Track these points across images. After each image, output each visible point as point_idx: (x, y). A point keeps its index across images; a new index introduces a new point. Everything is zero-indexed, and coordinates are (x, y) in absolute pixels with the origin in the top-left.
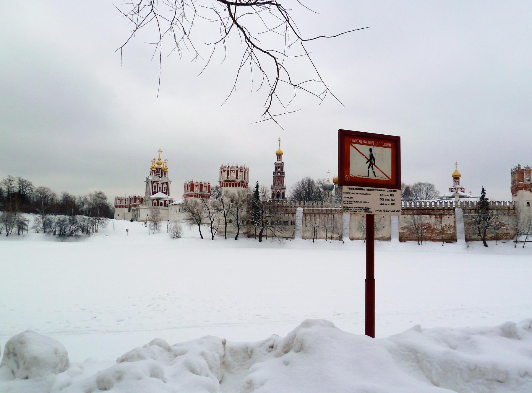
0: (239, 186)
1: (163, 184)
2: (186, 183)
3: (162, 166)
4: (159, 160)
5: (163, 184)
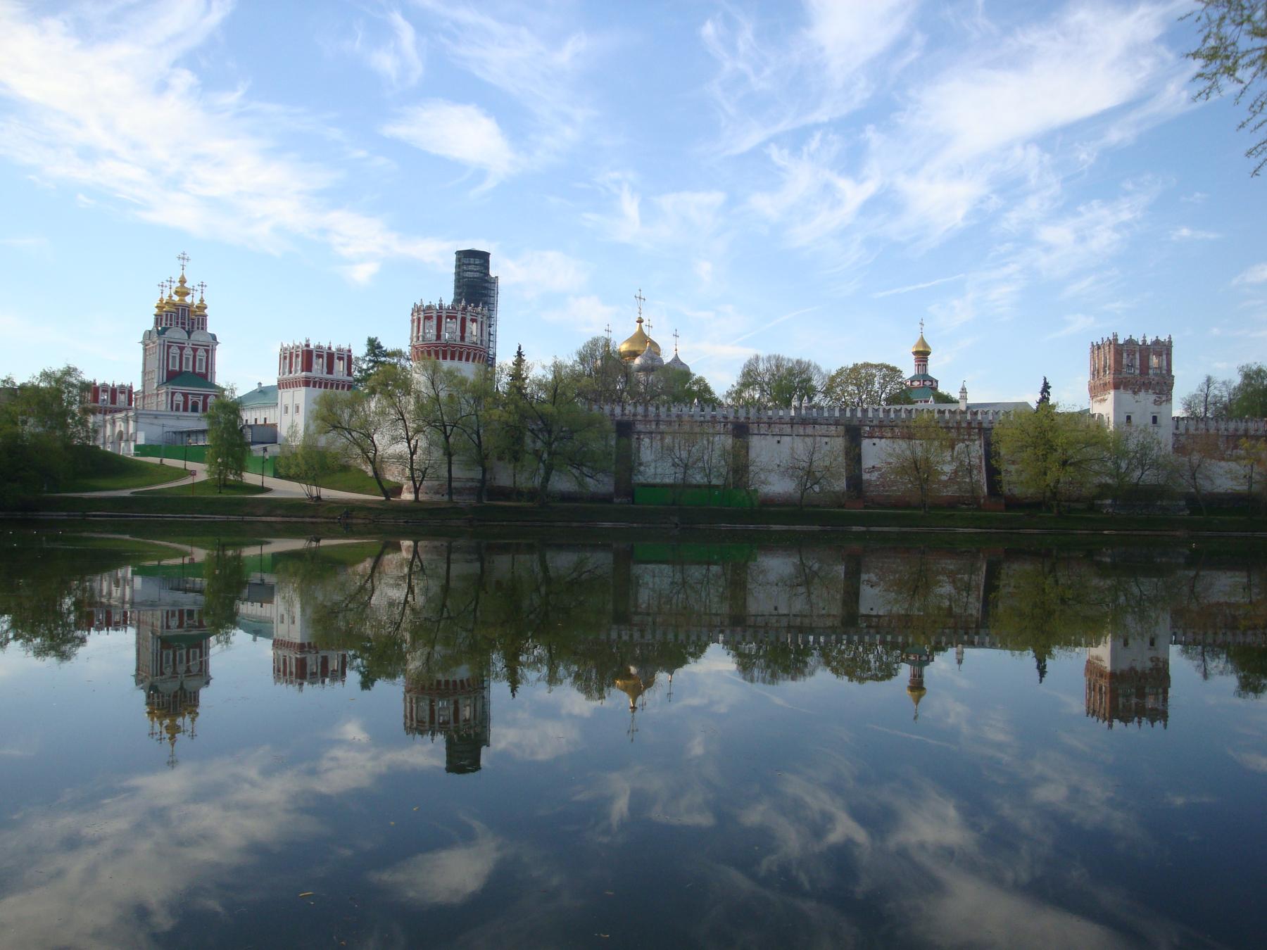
0: (467, 360)
1: (195, 350)
2: (284, 350)
3: (188, 299)
4: (183, 281)
5: (195, 350)
